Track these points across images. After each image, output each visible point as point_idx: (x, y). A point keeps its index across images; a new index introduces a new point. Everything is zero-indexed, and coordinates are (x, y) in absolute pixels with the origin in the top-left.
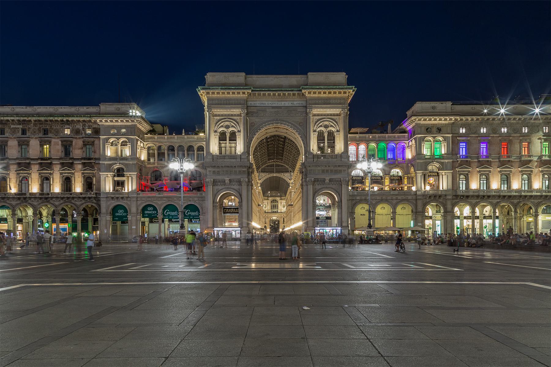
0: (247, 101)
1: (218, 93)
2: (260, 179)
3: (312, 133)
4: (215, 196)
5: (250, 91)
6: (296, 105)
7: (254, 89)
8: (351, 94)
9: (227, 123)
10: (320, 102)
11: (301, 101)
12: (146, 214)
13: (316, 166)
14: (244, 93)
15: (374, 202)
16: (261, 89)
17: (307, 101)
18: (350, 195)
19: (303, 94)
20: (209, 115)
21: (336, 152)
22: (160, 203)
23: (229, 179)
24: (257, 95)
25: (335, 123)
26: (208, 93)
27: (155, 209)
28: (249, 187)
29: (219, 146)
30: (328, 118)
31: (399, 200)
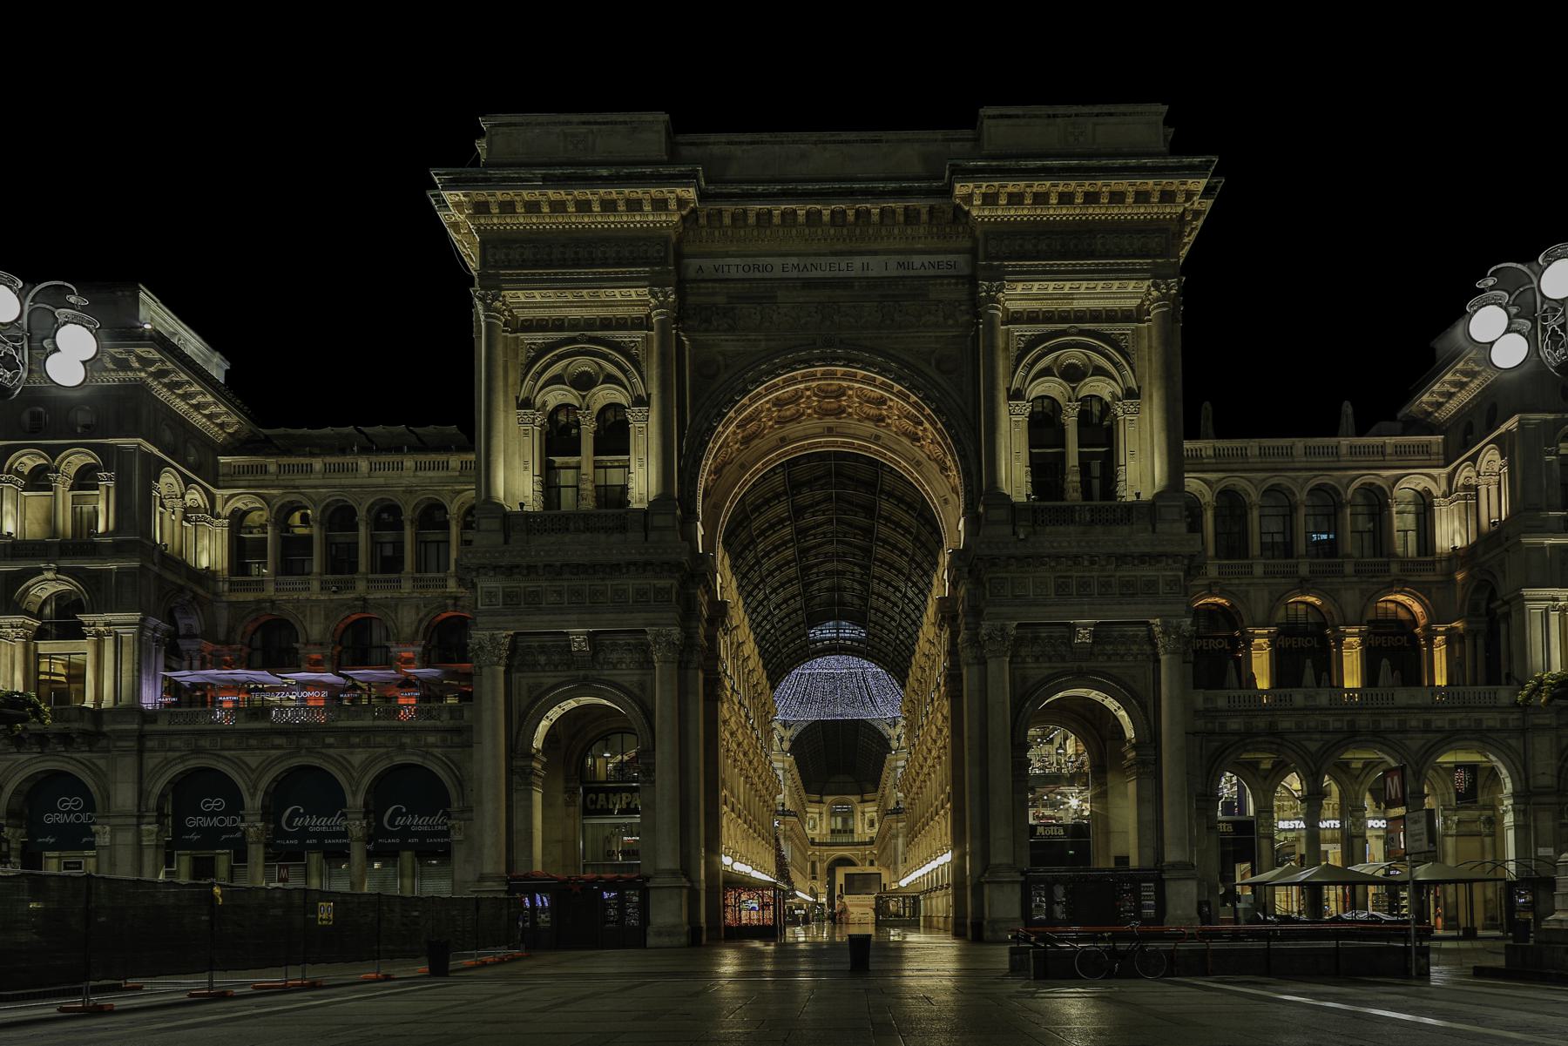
3: (1003, 409)
6: (922, 272)
8: (1197, 214)
15: (1313, 747)
22: (253, 760)
24: (727, 221)
25: (1118, 357)
30: (1082, 333)
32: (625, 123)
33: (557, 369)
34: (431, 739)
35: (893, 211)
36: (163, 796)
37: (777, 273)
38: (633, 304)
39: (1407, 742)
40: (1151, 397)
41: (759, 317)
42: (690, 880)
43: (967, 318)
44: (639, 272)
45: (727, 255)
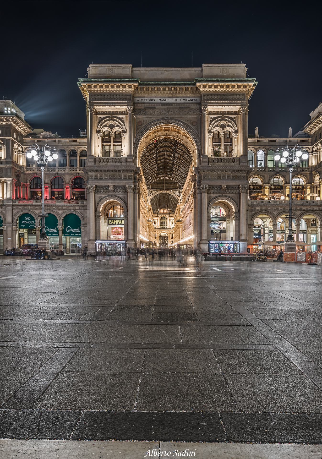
0: (134, 97)
1: (101, 87)
2: (150, 196)
3: (207, 134)
4: (97, 205)
5: (137, 84)
6: (189, 102)
7: (141, 83)
8: (252, 89)
9: (111, 122)
10: (216, 97)
11: (195, 97)
12: (23, 224)
13: (211, 171)
14: (130, 87)
16: (149, 82)
17: (201, 97)
18: (249, 205)
19: (197, 88)
20: (91, 112)
21: (234, 156)
23: (114, 186)
24: (145, 89)
25: (233, 123)
26: (90, 87)
27: (33, 219)
28: (135, 194)
29: (102, 148)
30: (225, 117)
31: (304, 211)
32: (122, 66)
33: (106, 123)
34: (77, 208)
35: (183, 88)
36: (17, 219)
37: (156, 102)
38: (123, 109)
39: (296, 213)
40: (240, 132)
41: (152, 112)
42: (135, 241)
43: (199, 113)
44: (125, 102)
45: (144, 97)
